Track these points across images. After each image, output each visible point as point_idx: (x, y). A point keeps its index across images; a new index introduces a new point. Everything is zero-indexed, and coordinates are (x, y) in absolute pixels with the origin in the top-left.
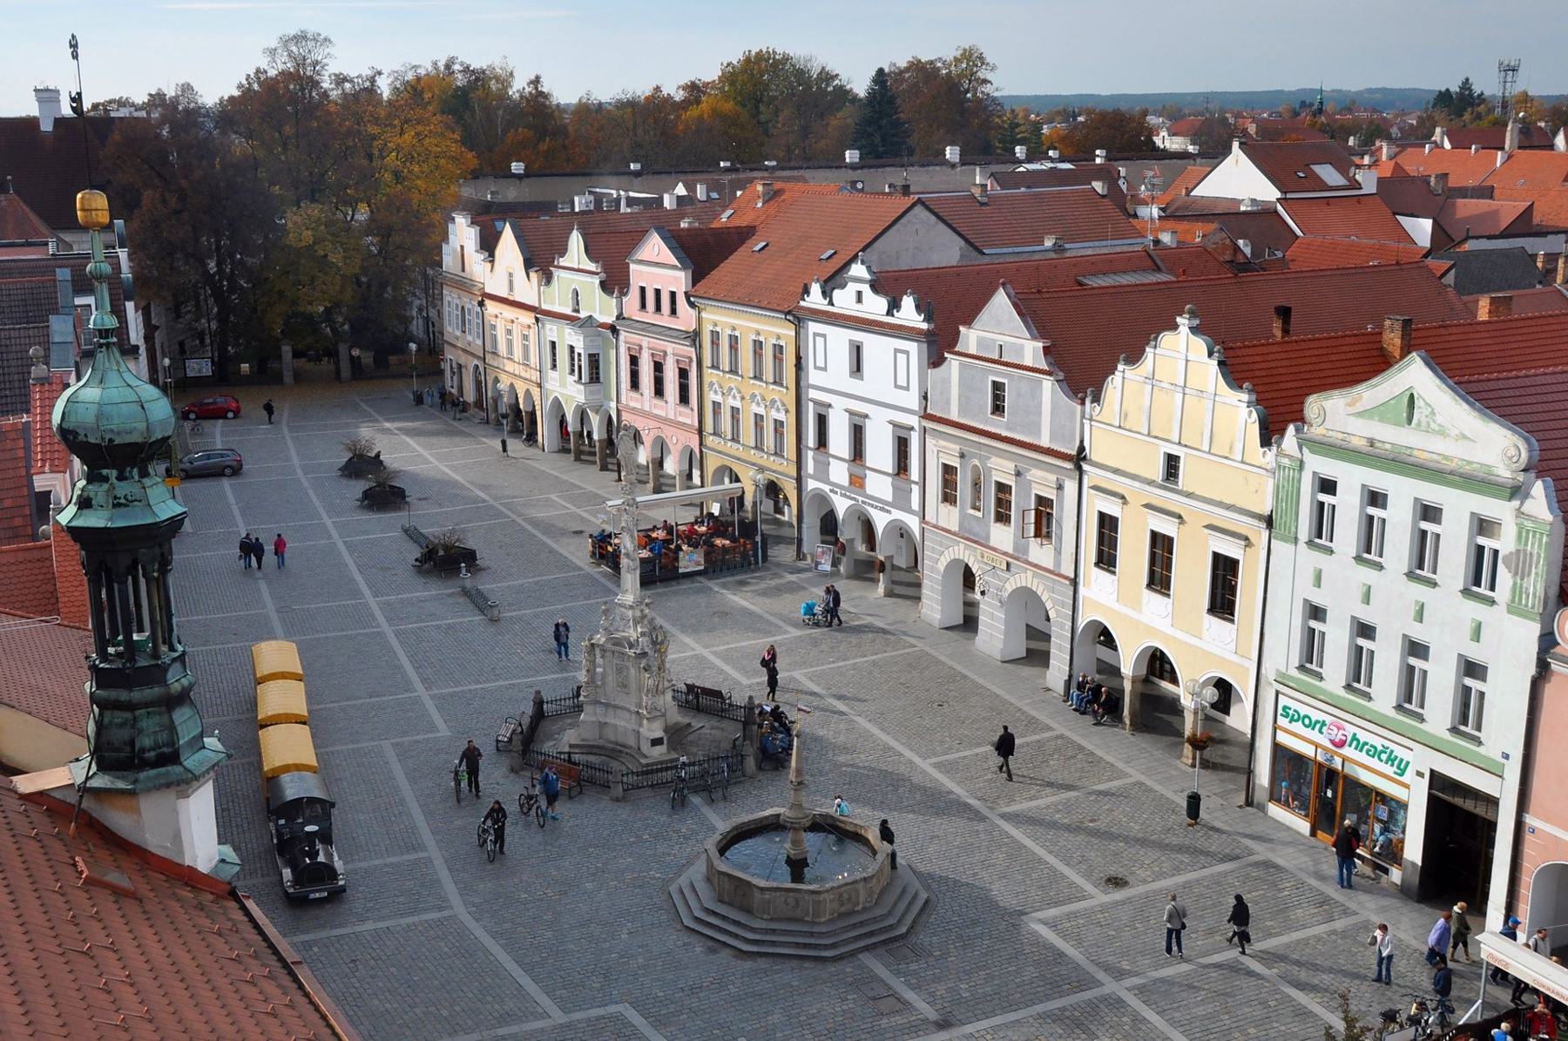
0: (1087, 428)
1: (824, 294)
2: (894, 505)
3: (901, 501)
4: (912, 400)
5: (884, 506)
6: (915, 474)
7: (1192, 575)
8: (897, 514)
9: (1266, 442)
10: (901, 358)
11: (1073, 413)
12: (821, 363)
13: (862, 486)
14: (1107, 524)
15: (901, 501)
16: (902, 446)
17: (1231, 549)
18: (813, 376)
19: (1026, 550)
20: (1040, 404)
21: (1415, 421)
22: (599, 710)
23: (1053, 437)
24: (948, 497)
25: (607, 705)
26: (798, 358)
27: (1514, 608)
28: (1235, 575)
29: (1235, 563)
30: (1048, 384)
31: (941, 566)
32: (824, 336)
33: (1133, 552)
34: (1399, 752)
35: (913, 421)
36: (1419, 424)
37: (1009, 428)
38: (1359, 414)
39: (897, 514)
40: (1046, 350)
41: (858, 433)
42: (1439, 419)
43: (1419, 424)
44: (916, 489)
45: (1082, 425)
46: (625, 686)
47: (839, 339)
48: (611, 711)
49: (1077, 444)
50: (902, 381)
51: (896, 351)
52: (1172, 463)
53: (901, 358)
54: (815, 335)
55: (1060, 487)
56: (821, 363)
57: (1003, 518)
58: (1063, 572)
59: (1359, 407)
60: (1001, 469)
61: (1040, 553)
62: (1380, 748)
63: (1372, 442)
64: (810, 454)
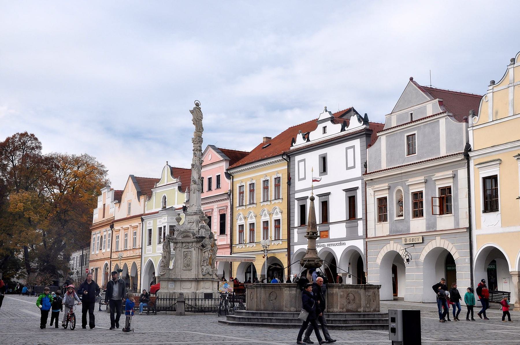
0: (471, 133)
1: (304, 138)
2: (347, 239)
3: (352, 235)
4: (358, 172)
5: (340, 241)
6: (360, 214)
8: (350, 243)
10: (350, 151)
11: (461, 129)
12: (302, 176)
13: (327, 236)
15: (352, 235)
16: (352, 202)
18: (298, 185)
19: (435, 224)
22: (171, 285)
24: (382, 217)
25: (174, 281)
26: (289, 179)
30: (443, 122)
31: (379, 260)
32: (304, 160)
35: (358, 184)
37: (418, 157)
39: (350, 243)
40: (441, 103)
41: (325, 205)
44: (360, 223)
45: (467, 132)
46: (188, 265)
47: (312, 159)
48: (178, 284)
49: (465, 144)
50: (351, 164)
51: (347, 149)
53: (350, 151)
54: (299, 162)
55: (454, 177)
56: (302, 176)
57: (418, 213)
60: (416, 183)
61: (445, 222)
64: (296, 231)
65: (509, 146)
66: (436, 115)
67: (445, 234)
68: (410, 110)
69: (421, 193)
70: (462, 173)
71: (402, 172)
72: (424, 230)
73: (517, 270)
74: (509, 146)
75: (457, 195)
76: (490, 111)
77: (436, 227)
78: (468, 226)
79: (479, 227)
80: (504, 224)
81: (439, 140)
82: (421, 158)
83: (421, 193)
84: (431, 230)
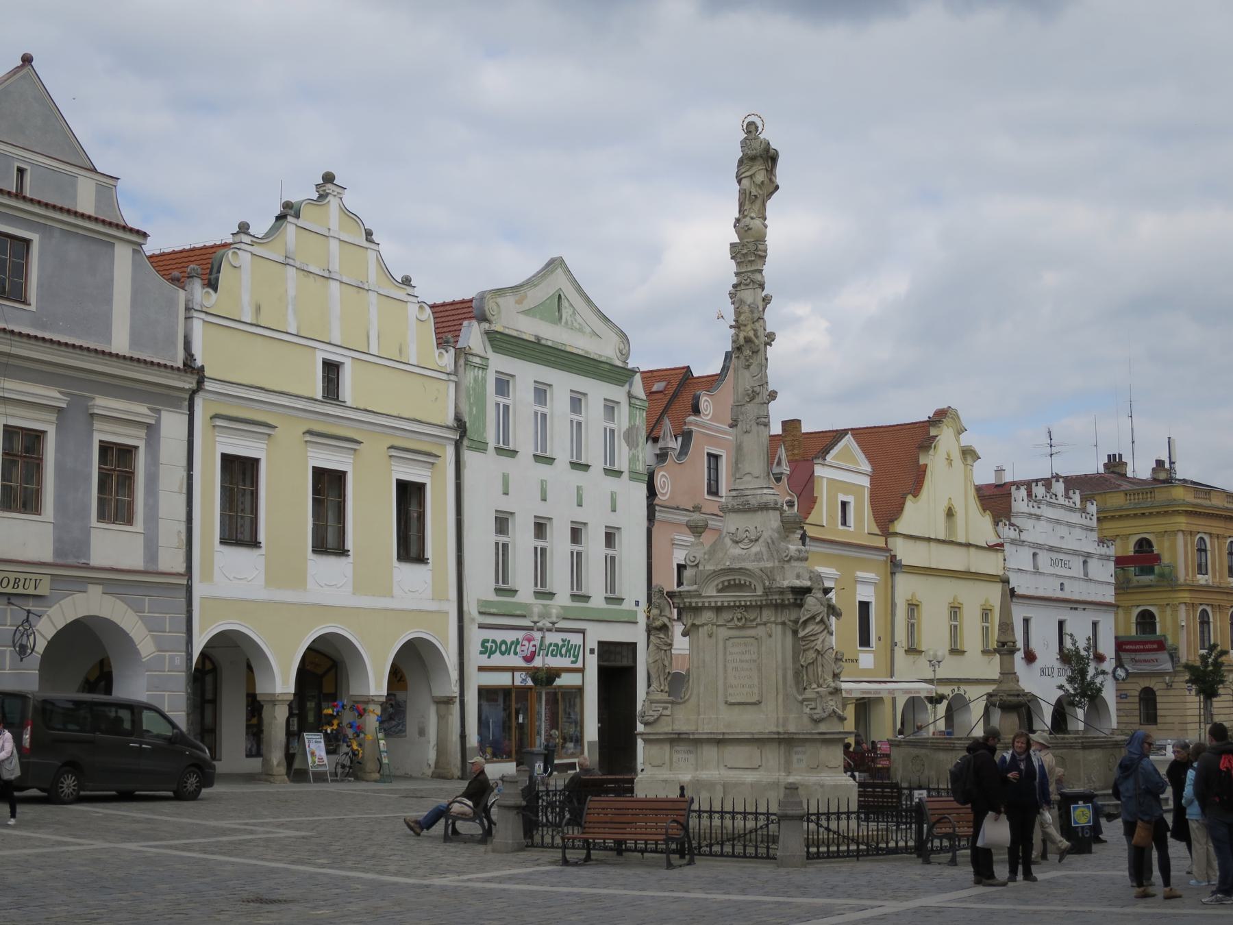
7: (370, 514)
9: (442, 343)
14: (240, 473)
17: (413, 474)
19: (83, 545)
20: (109, 283)
21: (564, 320)
23: (135, 340)
27: (634, 476)
28: (422, 503)
29: (421, 487)
33: (284, 503)
34: (576, 639)
36: (566, 323)
38: (526, 312)
42: (578, 317)
43: (566, 323)
52: (331, 370)
58: (163, 566)
59: (527, 305)
61: (113, 547)
62: (560, 643)
63: (538, 338)
65: (300, 404)
66: (103, 222)
67: (117, 581)
68: (21, 157)
69: (36, 437)
70: (172, 424)
71: (15, 351)
72: (48, 556)
73: (293, 691)
74: (300, 404)
75: (152, 480)
76: (246, 298)
77: (87, 554)
78: (181, 569)
79: (208, 576)
80: (272, 580)
81: (109, 300)
82: (44, 327)
83: (36, 437)
84: (71, 561)
